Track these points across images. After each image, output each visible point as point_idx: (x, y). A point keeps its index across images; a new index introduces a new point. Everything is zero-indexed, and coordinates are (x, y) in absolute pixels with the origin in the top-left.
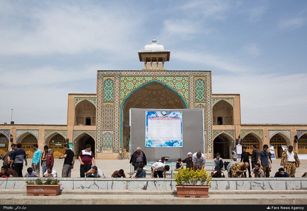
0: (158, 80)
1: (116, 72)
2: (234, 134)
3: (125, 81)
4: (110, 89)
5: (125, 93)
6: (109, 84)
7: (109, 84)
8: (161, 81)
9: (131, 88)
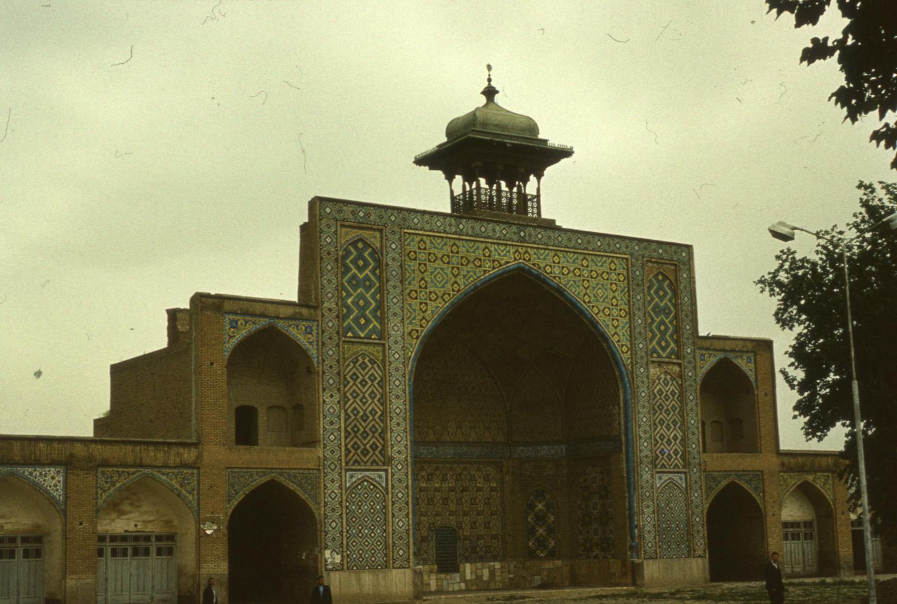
0: (534, 265)
8: (542, 265)
9: (443, 287)
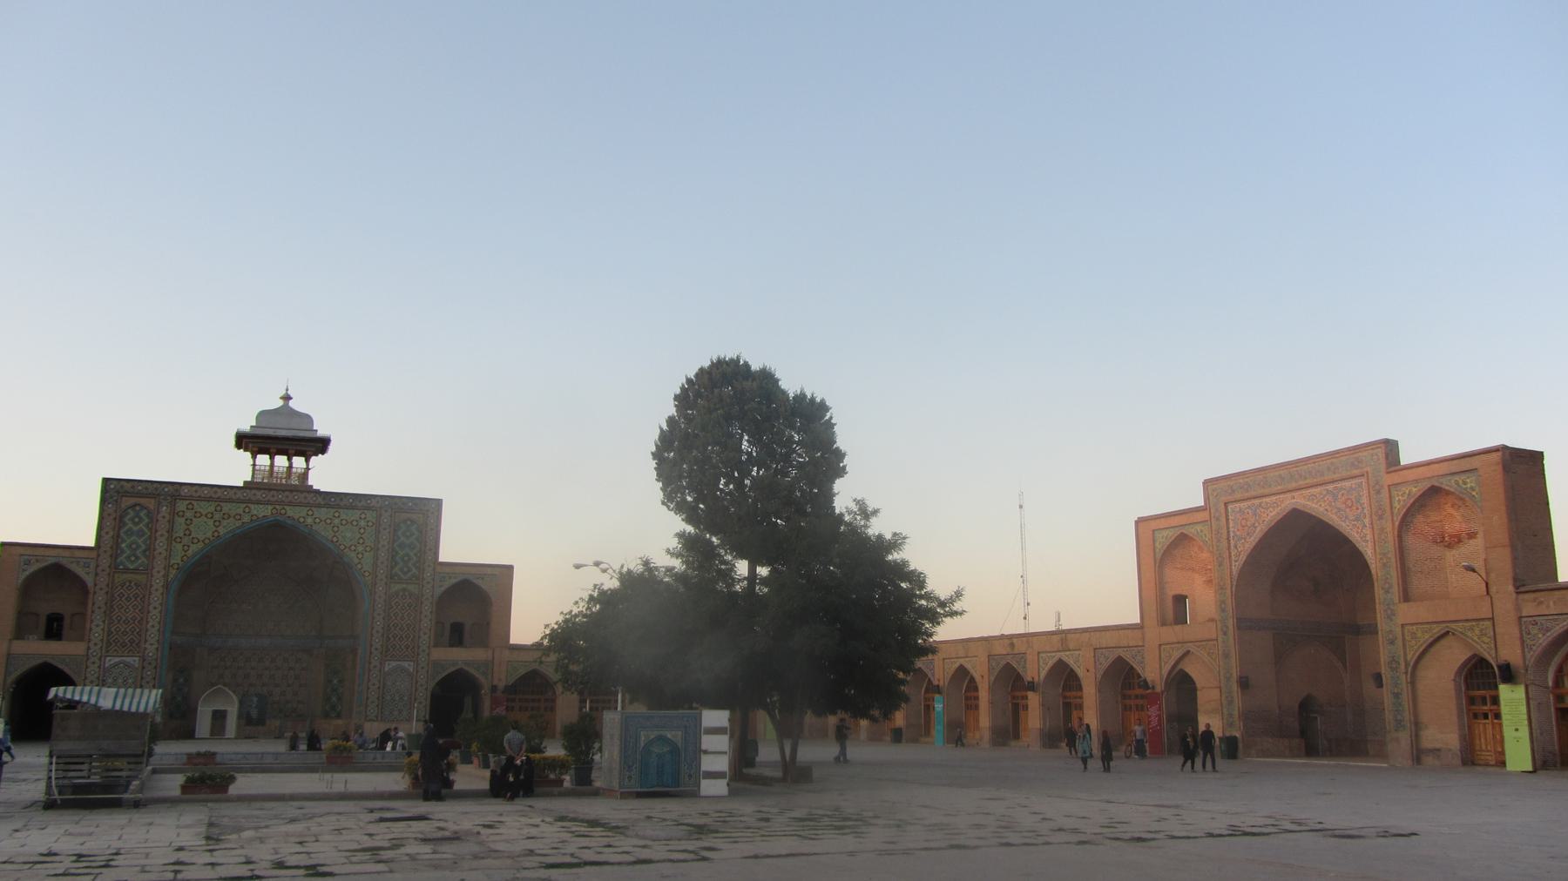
3: (189, 514)
4: (141, 534)
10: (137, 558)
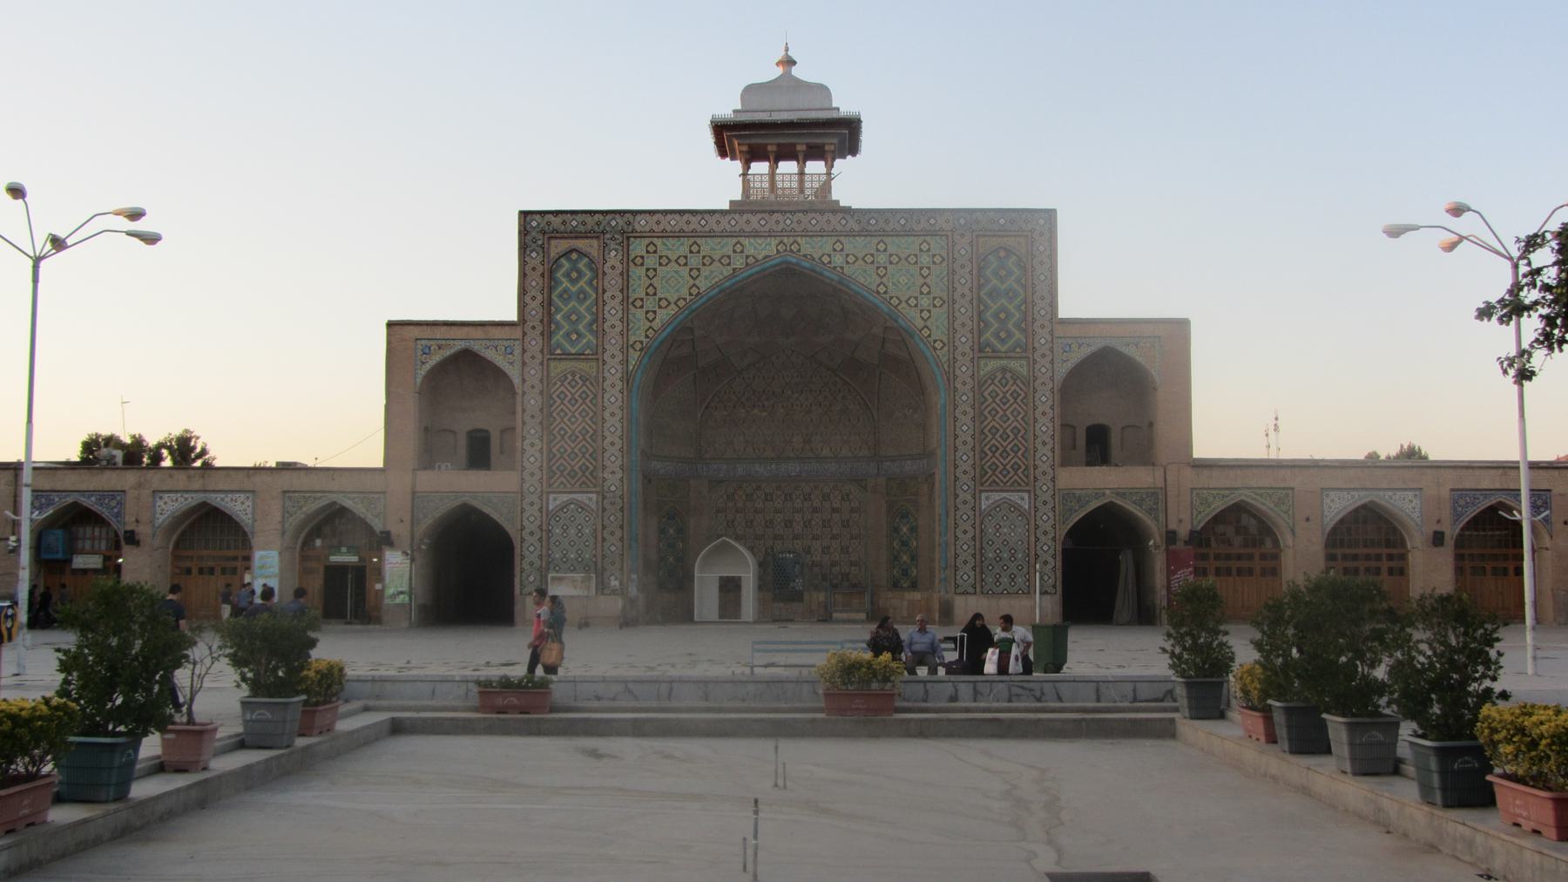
1: (609, 217)
2: (1161, 506)
4: (582, 296)
5: (651, 316)
6: (574, 275)
7: (574, 275)
10: (580, 335)
